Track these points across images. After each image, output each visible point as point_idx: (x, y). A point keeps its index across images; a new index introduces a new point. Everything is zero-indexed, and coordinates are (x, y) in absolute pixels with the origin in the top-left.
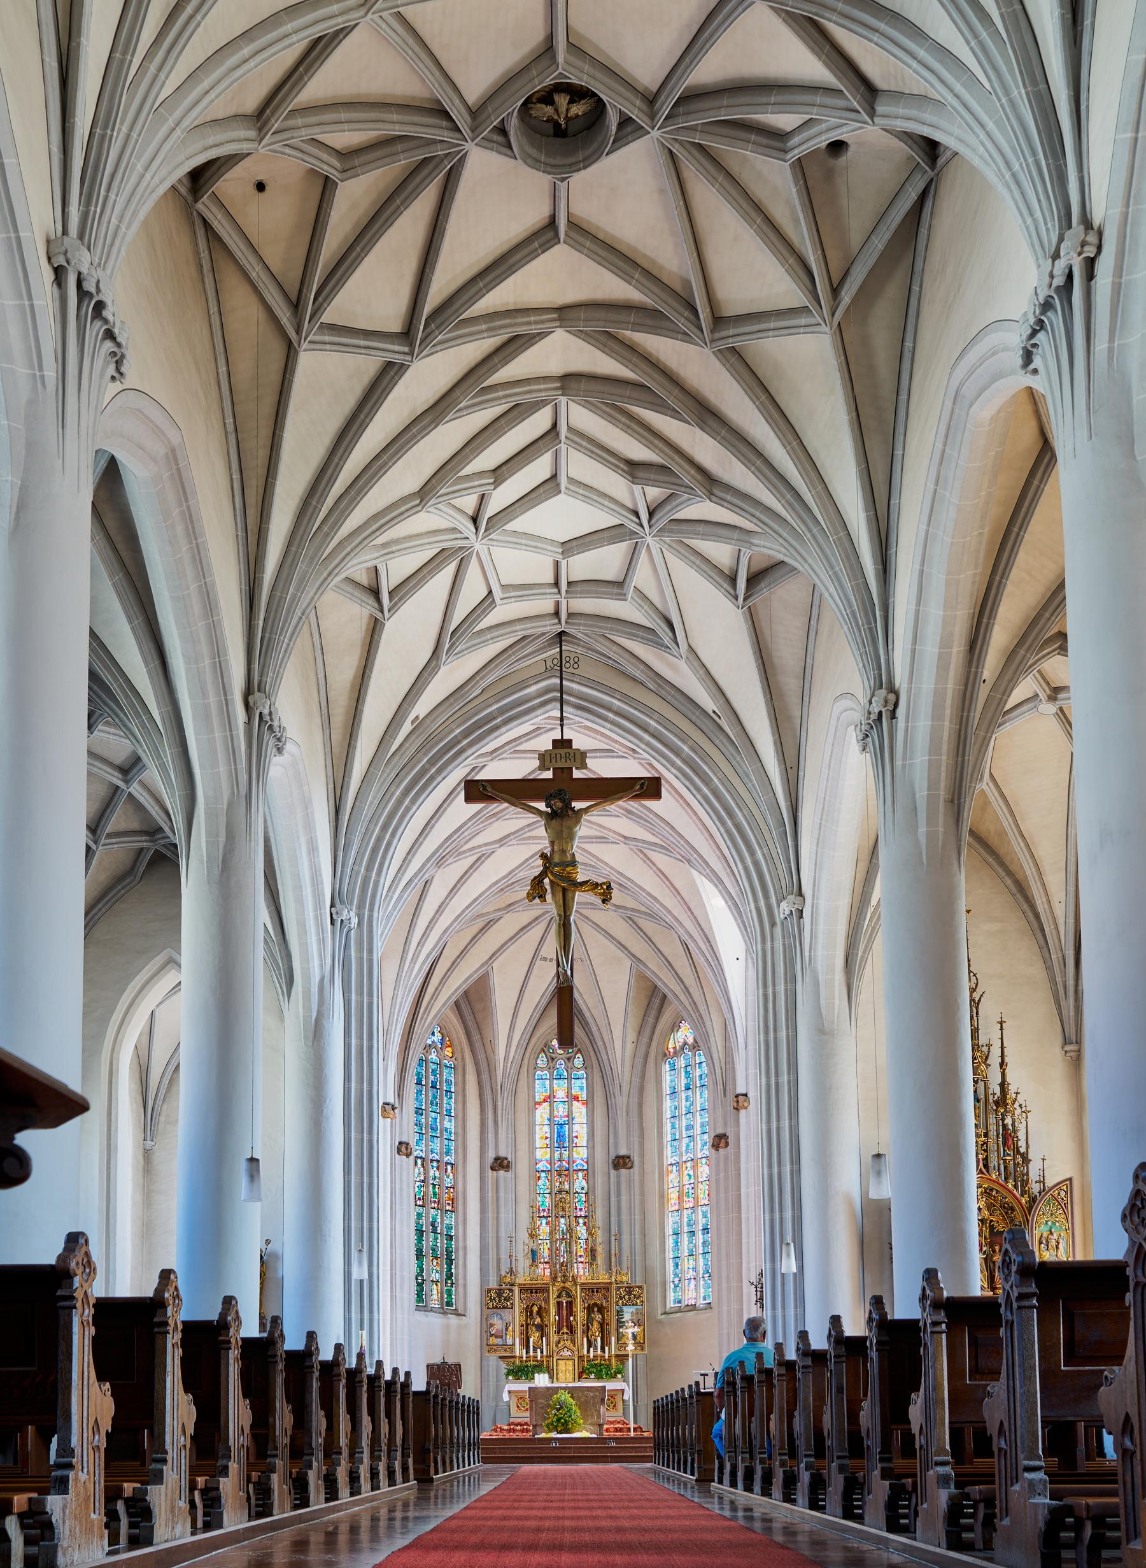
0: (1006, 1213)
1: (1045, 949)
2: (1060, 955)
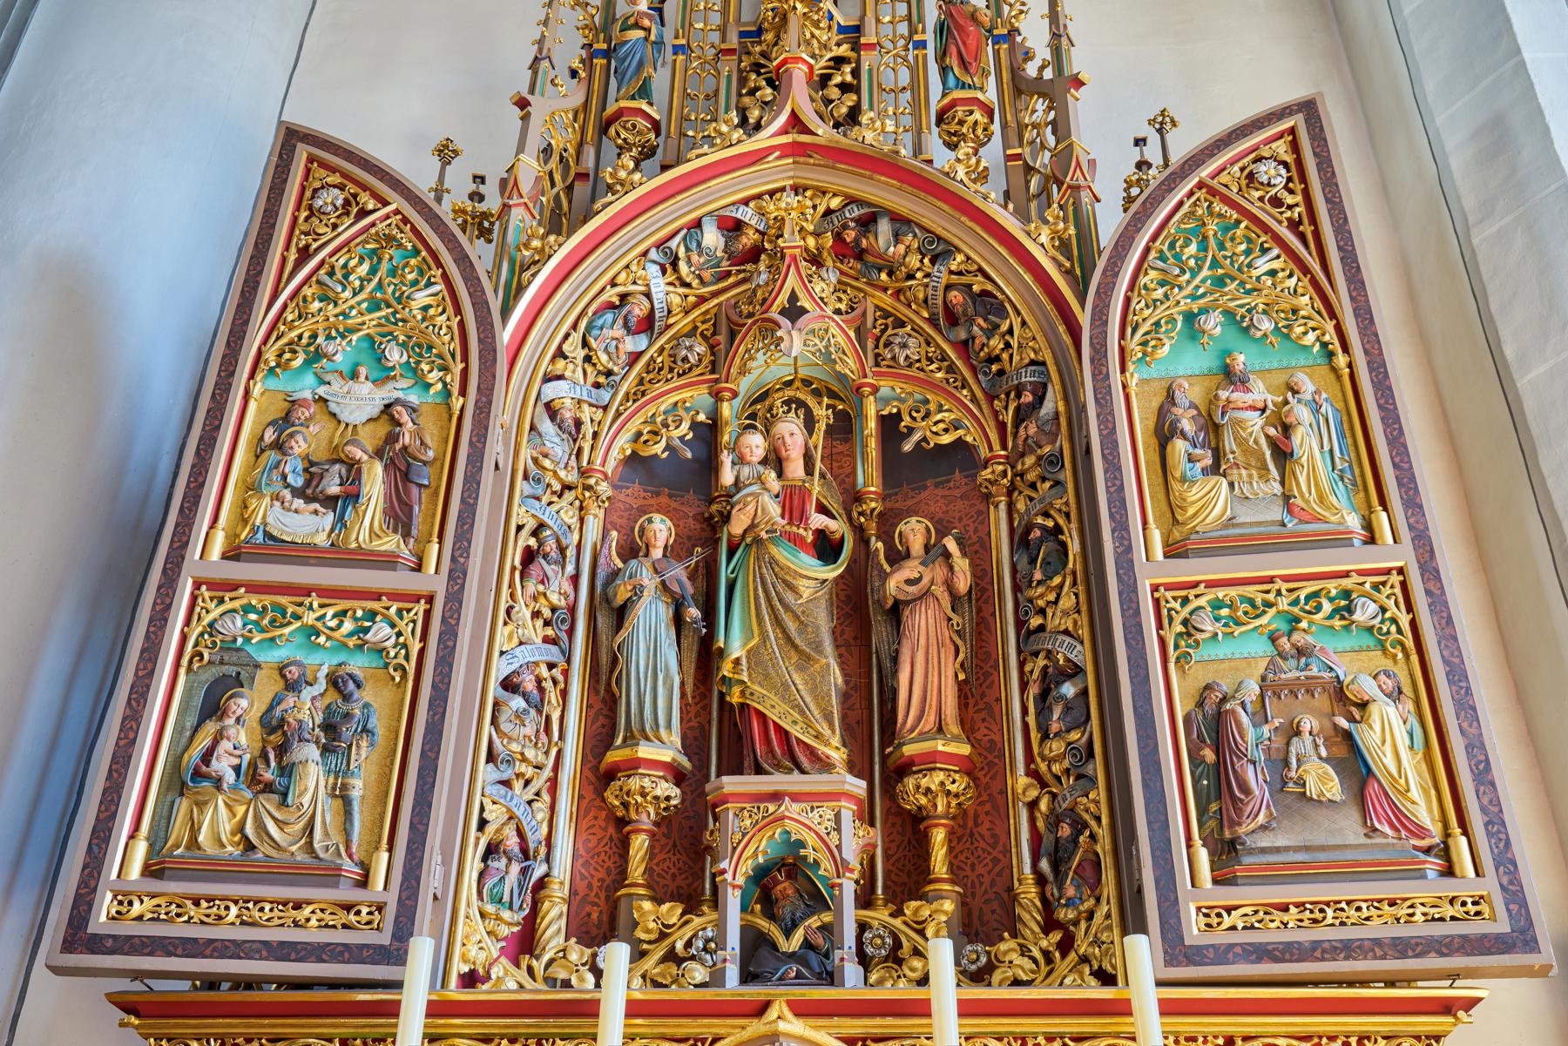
0: (964, 347)
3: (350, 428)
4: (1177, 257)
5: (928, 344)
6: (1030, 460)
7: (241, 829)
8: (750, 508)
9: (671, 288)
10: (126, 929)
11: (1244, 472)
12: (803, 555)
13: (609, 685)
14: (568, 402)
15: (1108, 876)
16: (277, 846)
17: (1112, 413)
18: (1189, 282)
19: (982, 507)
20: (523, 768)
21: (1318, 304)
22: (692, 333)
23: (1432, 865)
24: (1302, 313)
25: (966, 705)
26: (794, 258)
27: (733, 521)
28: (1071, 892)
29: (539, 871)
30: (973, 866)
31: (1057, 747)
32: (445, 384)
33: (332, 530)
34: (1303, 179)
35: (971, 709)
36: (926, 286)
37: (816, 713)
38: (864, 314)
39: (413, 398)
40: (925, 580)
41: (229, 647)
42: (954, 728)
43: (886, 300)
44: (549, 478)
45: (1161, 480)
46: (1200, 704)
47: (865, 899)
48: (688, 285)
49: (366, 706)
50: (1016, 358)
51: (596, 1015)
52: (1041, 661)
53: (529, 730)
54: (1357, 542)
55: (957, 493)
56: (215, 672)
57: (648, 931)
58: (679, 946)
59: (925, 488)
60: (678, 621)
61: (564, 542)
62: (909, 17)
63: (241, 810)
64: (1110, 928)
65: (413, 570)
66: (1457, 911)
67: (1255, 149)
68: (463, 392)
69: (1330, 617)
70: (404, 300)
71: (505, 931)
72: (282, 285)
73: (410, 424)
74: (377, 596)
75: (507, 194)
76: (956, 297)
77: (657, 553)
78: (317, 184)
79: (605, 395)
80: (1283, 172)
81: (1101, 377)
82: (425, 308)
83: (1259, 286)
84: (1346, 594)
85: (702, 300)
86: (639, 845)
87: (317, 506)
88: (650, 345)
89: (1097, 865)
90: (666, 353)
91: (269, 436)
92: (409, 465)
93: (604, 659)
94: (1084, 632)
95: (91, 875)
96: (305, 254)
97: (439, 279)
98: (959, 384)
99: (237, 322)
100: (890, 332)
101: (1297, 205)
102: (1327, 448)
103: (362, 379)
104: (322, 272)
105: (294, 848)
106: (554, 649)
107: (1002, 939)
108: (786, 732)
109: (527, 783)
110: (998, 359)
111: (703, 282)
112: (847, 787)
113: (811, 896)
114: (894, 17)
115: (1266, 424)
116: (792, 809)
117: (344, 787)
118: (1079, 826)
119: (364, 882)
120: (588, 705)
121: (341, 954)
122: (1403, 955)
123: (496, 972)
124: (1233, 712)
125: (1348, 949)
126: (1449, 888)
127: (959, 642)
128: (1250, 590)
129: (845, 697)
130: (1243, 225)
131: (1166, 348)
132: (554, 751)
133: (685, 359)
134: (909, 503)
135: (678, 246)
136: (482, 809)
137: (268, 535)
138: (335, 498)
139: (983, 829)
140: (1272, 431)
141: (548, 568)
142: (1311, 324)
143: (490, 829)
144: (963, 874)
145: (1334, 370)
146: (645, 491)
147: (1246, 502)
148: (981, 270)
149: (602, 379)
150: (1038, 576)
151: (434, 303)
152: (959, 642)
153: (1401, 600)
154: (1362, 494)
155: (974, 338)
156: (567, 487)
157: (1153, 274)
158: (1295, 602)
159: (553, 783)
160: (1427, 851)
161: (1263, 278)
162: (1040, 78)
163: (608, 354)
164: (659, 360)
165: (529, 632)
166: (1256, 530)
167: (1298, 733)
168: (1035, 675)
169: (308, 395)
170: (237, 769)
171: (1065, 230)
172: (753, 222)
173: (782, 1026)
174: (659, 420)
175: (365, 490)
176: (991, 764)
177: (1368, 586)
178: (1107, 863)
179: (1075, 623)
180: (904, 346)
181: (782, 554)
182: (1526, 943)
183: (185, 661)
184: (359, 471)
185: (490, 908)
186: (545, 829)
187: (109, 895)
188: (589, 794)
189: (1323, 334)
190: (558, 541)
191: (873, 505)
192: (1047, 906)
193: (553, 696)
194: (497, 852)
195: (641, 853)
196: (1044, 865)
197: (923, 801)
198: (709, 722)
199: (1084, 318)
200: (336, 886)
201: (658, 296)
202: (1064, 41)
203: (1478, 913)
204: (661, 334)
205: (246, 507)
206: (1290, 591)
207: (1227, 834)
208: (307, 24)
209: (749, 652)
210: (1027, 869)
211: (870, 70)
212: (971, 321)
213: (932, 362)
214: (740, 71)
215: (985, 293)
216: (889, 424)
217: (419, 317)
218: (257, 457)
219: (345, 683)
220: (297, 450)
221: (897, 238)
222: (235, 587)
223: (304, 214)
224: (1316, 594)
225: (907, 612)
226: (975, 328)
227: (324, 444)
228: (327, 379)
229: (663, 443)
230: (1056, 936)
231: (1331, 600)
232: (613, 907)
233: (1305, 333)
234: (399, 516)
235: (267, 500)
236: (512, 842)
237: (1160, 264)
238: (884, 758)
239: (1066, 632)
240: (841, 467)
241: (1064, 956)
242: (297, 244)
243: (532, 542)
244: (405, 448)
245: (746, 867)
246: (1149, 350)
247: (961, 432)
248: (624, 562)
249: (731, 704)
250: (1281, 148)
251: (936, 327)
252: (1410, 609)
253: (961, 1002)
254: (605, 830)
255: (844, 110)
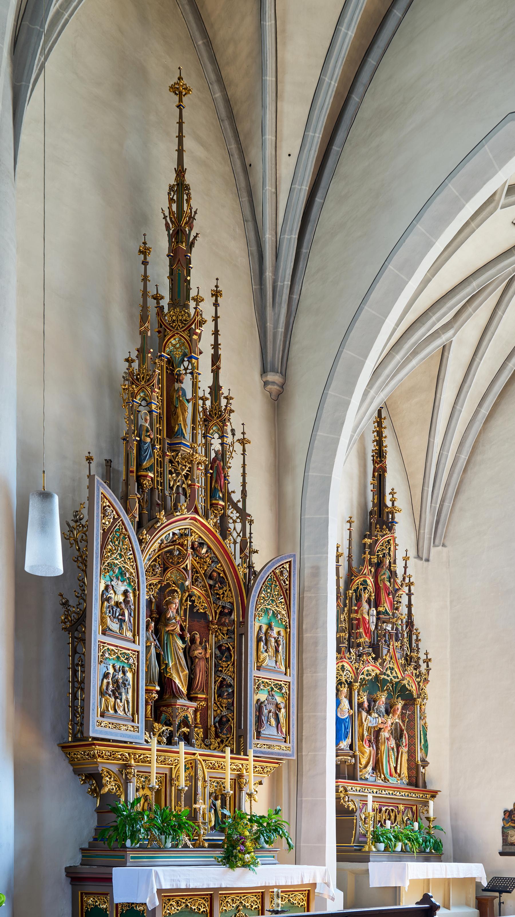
76: (215, 574)
110: (219, 595)
226: (217, 585)
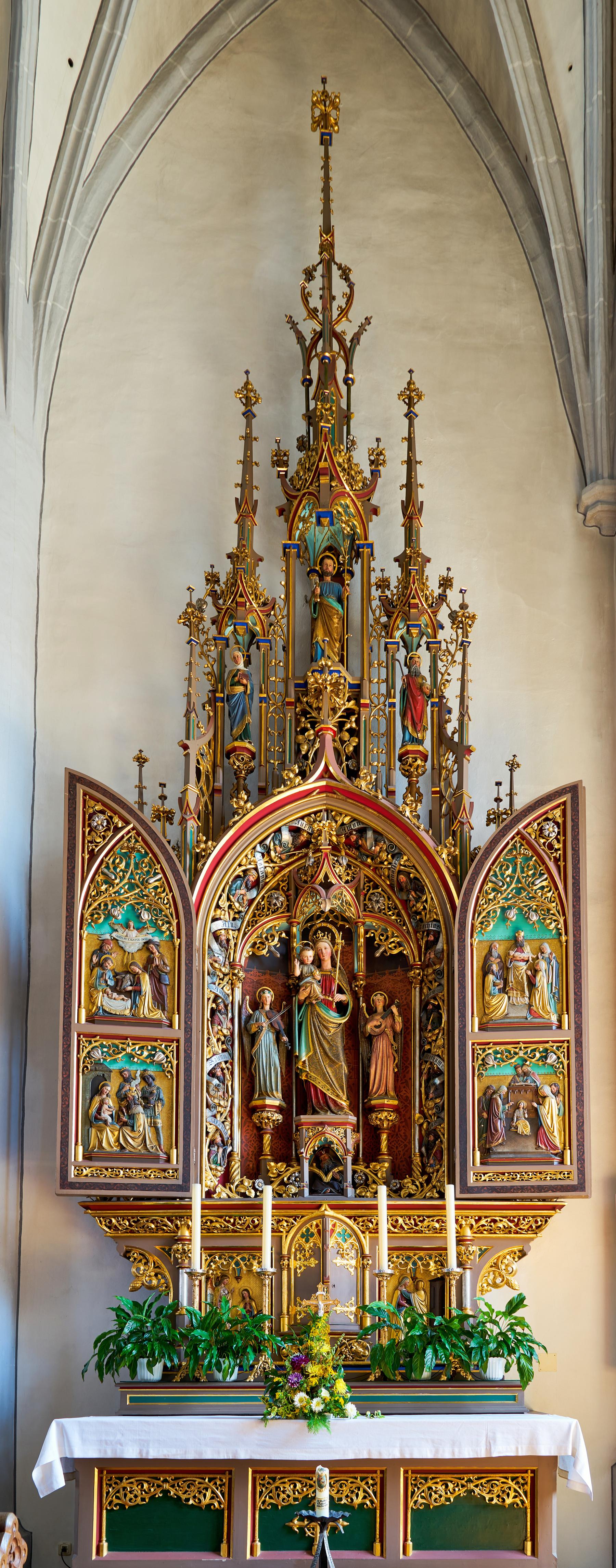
0: (405, 903)
1: (542, 260)
2: (573, 247)
3: (130, 955)
4: (502, 875)
5: (389, 899)
6: (430, 971)
7: (118, 1140)
8: (308, 990)
9: (267, 865)
10: (82, 1179)
11: (515, 992)
12: (331, 1012)
13: (250, 1068)
14: (223, 932)
15: (445, 1157)
16: (134, 1148)
17: (464, 959)
18: (505, 890)
19: (409, 987)
20: (220, 1109)
21: (559, 907)
22: (276, 888)
23: (556, 1160)
24: (551, 912)
25: (398, 1080)
26: (326, 855)
27: (301, 994)
28: (432, 1162)
29: (229, 1149)
30: (397, 1147)
31: (431, 1104)
32: (170, 932)
33: (131, 1009)
34: (565, 835)
35: (400, 1082)
36: (389, 869)
37: (337, 1085)
38: (359, 880)
39: (156, 939)
40: (383, 1026)
41: (97, 1063)
42: (392, 1093)
43: (370, 873)
44: (218, 973)
45: (481, 992)
46: (485, 1094)
47: (355, 1161)
48: (276, 863)
49: (158, 1088)
50: (428, 916)
51: (262, 1209)
52: (428, 1065)
53: (221, 1093)
54: (554, 1028)
55: (399, 978)
56: (94, 1074)
57: (273, 1174)
58: (285, 1179)
59: (385, 974)
60: (278, 1040)
61: (226, 1002)
62: (387, 680)
63: (116, 1133)
64: (444, 1176)
65: (168, 1026)
66: (562, 1176)
67: (546, 812)
68: (179, 936)
69: (538, 1060)
70: (145, 883)
71: (219, 1174)
72: (85, 874)
73: (157, 953)
74: (156, 1040)
75: (184, 811)
76: (402, 878)
77: (267, 1008)
78: (91, 811)
79: (239, 923)
80: (556, 830)
81: (462, 940)
82: (156, 888)
83: (536, 896)
84: (546, 1050)
85: (282, 868)
86: (267, 1138)
87: (123, 996)
88: (258, 894)
89: (442, 1152)
90: (265, 899)
91: (95, 960)
92: (160, 975)
93: (248, 1058)
94: (445, 1057)
95: (64, 1159)
96: (93, 856)
97: (159, 871)
98: (402, 923)
99: (69, 897)
100: (371, 891)
101: (559, 849)
102: (550, 982)
103: (132, 928)
104: (103, 867)
105: (139, 1148)
106: (226, 1054)
107: (406, 1178)
108: (325, 1094)
109: (221, 1114)
110: (420, 913)
111: (282, 860)
112: (349, 1120)
113: (334, 1158)
114: (379, 679)
115: (527, 969)
116: (328, 1129)
117: (155, 1123)
118: (437, 1137)
119: (168, 1160)
120: (242, 1078)
121: (165, 1188)
122: (540, 1192)
123: (218, 1190)
124: (496, 1099)
125: (522, 1189)
126: (561, 1168)
127: (396, 1055)
128: (509, 1047)
129: (349, 1078)
130: (534, 858)
131: (491, 926)
132: (230, 1099)
133: (275, 905)
134: (377, 981)
135: (270, 843)
136: (207, 1128)
137: (104, 1011)
138: (130, 992)
139: (402, 1133)
140: (529, 973)
141: (221, 1017)
142: (555, 918)
143: (210, 1135)
144: (393, 1150)
145: (560, 942)
146: (259, 972)
147: (514, 1007)
148: (414, 866)
149: (237, 916)
150: (429, 1027)
151: (159, 885)
152: (396, 1055)
153: (566, 1054)
154: (560, 1004)
155: (410, 901)
156: (225, 975)
157: (490, 884)
158: (526, 1053)
159: (231, 1112)
160: (556, 1155)
161: (538, 891)
162: (452, 739)
163: (239, 903)
164: (263, 903)
165: (216, 1049)
166: (516, 1020)
167: (518, 1108)
168: (425, 1071)
169: (108, 937)
170: (111, 1116)
171: (455, 851)
172: (306, 829)
173: (326, 1213)
174: (264, 936)
175: (143, 988)
176: (406, 1106)
177: (554, 1048)
178: (445, 1152)
179: (442, 1052)
180: (377, 902)
181: (322, 1011)
182: (581, 1188)
183: (81, 1070)
184: (139, 978)
185: (213, 1166)
186: (229, 1132)
187: (73, 1167)
188: (245, 1117)
189: (558, 924)
190: (224, 1003)
191: (362, 982)
192: (424, 1166)
193: (228, 1076)
194: (213, 1144)
195: (268, 1142)
196: (423, 1149)
197: (379, 1123)
198: (292, 1083)
199: (458, 902)
200: (158, 1162)
201: (261, 869)
202: (466, 718)
203: (568, 1177)
204: (263, 888)
205: (92, 996)
206: (525, 1048)
207: (487, 1146)
208: (36, 636)
209: (309, 1057)
210: (417, 1151)
211: (365, 721)
212: (408, 892)
213: (390, 910)
214: (296, 714)
215: (415, 878)
216: (369, 942)
217: (153, 894)
218: (92, 971)
219: (148, 1079)
220: (109, 967)
221: (376, 842)
222: (95, 1036)
223: (87, 830)
224: (534, 1050)
225: (375, 1040)
227: (120, 963)
228: (116, 928)
229: (266, 950)
230: (425, 1177)
231: (540, 1053)
232: (258, 1163)
233: (551, 923)
234: (159, 1001)
235: (101, 993)
236: (219, 1139)
237: (494, 879)
238: (363, 1103)
239: (438, 1056)
240: (347, 959)
241: (427, 1185)
242: (88, 849)
243: (214, 1006)
244: (157, 966)
245: (310, 1151)
246: (484, 926)
247: (402, 948)
248: (253, 1011)
249: (301, 1080)
250: (558, 813)
251: (393, 890)
252: (568, 1059)
253: (388, 1205)
254: (253, 1131)
255: (351, 749)
